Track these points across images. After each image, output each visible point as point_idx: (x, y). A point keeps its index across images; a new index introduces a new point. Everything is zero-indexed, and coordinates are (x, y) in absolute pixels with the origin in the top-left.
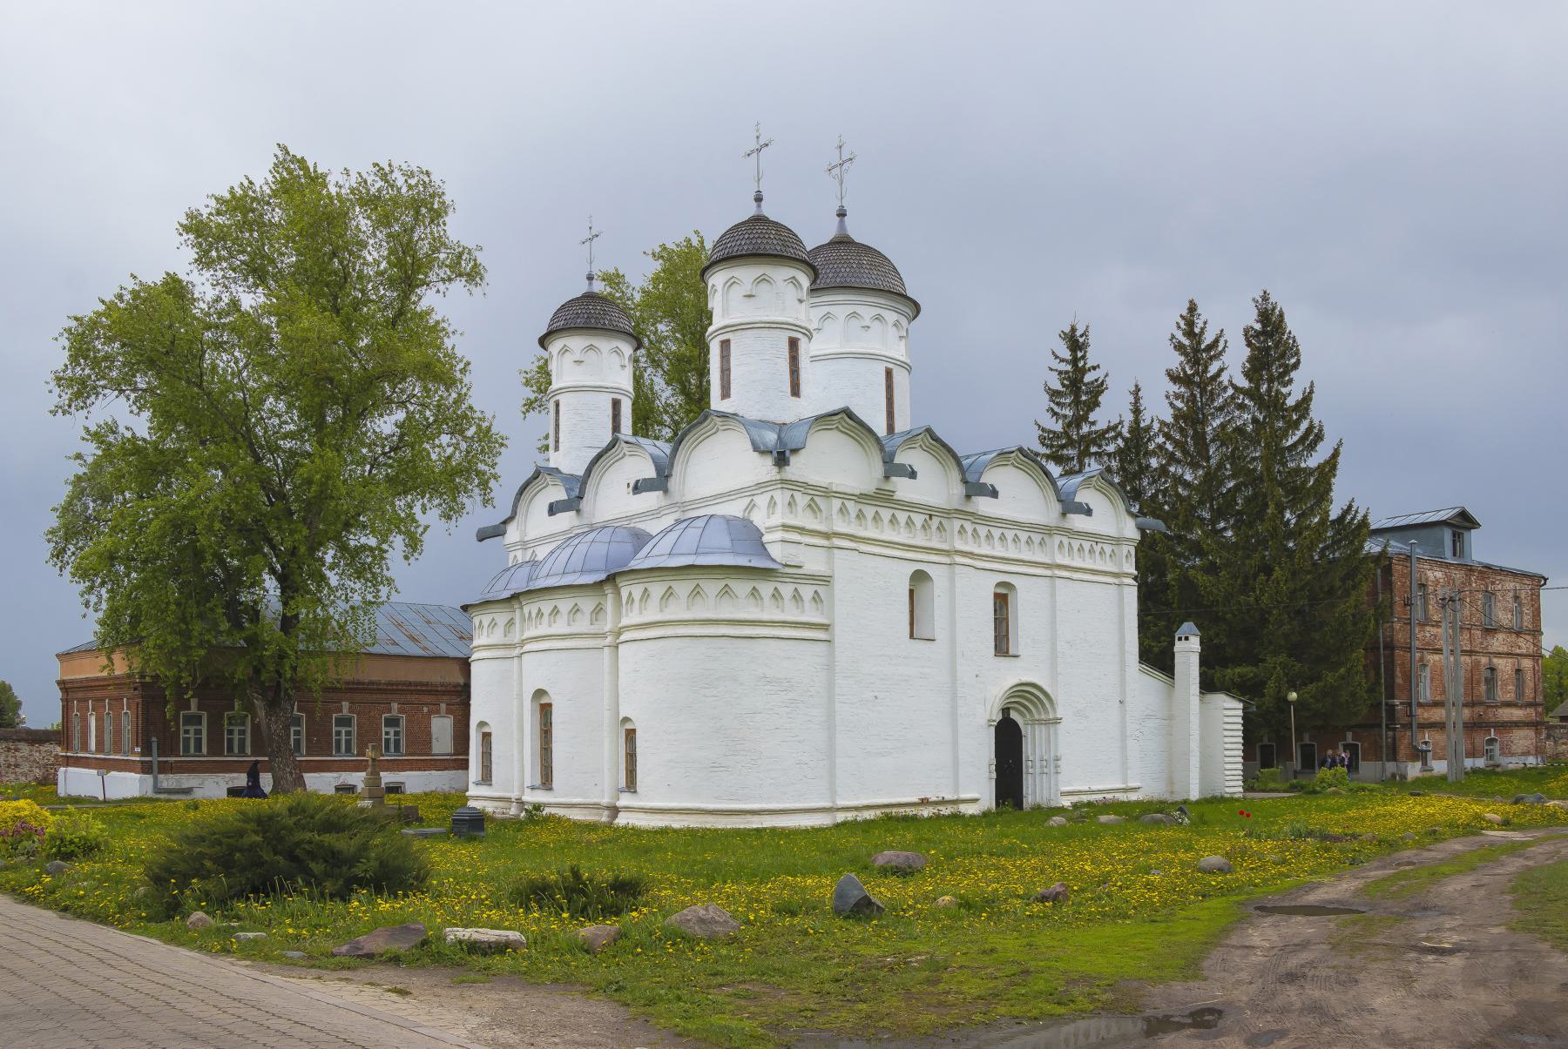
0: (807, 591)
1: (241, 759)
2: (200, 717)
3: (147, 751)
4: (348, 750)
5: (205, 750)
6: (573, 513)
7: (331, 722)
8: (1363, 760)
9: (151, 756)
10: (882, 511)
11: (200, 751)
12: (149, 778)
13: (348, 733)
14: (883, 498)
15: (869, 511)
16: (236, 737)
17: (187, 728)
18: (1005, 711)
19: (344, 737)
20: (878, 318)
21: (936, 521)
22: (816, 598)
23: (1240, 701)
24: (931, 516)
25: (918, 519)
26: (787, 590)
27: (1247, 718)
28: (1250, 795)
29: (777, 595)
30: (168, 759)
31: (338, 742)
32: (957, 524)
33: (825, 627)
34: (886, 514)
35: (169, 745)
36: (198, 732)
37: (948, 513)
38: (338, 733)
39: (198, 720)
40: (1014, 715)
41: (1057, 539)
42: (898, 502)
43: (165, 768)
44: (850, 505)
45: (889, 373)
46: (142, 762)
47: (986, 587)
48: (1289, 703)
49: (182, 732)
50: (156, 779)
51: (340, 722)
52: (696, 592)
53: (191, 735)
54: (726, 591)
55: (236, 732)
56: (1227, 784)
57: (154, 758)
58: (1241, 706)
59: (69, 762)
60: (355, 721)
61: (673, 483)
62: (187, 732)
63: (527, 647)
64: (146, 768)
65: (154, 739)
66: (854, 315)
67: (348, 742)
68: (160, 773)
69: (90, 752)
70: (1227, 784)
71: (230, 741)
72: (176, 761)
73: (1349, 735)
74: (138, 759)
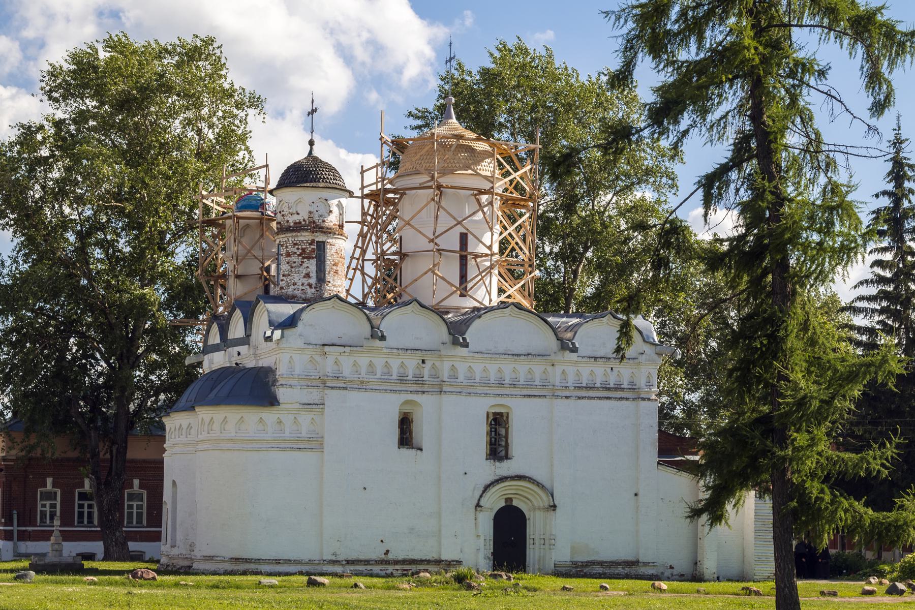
1: (88, 529)
2: (55, 493)
4: (139, 520)
5: (145, 522)
6: (247, 346)
9: (12, 525)
11: (83, 522)
12: (10, 544)
16: (86, 510)
17: (131, 503)
19: (135, 511)
21: (428, 364)
24: (423, 362)
30: (28, 528)
36: (53, 506)
38: (130, 507)
43: (23, 536)
46: (5, 531)
47: (481, 408)
50: (15, 544)
53: (48, 509)
62: (44, 506)
63: (200, 447)
65: (15, 512)
68: (19, 540)
69: (144, 527)
71: (81, 515)
72: (33, 530)
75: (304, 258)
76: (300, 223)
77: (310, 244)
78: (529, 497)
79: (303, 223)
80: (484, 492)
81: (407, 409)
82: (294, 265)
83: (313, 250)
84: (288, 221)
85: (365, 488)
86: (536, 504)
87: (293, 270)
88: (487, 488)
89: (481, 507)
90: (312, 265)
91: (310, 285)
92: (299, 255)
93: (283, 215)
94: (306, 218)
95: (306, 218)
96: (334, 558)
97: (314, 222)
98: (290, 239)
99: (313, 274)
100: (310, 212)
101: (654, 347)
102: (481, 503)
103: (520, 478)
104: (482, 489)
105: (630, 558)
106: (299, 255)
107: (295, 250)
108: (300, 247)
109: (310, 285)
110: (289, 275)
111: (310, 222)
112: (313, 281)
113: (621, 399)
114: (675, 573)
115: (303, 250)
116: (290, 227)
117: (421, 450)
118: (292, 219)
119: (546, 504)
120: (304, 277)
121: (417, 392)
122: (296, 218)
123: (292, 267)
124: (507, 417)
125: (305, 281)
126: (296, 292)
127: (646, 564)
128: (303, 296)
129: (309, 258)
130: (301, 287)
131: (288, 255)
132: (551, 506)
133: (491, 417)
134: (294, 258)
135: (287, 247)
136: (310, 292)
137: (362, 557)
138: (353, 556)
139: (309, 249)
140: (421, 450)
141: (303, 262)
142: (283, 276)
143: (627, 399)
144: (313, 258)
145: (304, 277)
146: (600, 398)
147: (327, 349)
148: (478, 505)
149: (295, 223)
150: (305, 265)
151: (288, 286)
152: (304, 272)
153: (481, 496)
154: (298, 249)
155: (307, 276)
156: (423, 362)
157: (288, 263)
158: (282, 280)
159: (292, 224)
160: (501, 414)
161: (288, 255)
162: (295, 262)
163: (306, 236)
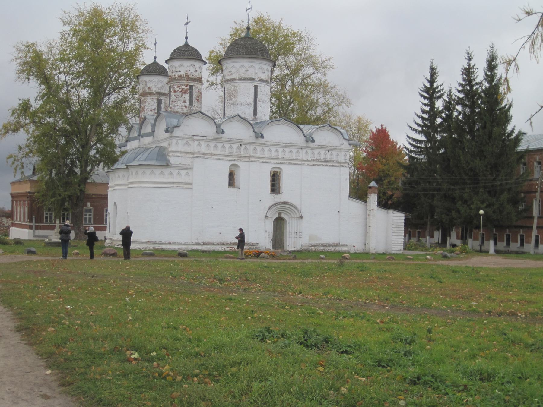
0: (183, 172)
3: (31, 221)
5: (92, 222)
7: (104, 211)
8: (486, 241)
10: (218, 144)
13: (90, 215)
14: (216, 139)
15: (212, 144)
18: (280, 214)
20: (252, 66)
21: (243, 147)
22: (187, 174)
23: (403, 213)
24: (241, 145)
25: (235, 146)
26: (175, 172)
27: (406, 220)
28: (407, 252)
29: (171, 174)
31: (86, 219)
32: (252, 147)
33: (191, 184)
34: (220, 145)
35: (39, 219)
37: (250, 143)
39: (90, 211)
40: (283, 216)
41: (304, 151)
42: (226, 141)
44: (202, 143)
45: (256, 87)
48: (480, 215)
49: (45, 214)
51: (86, 211)
52: (144, 173)
54: (152, 172)
55: (49, 214)
56: (393, 246)
57: (33, 224)
58: (404, 215)
59: (14, 225)
60: (93, 210)
61: (155, 133)
64: (30, 228)
66: (242, 66)
67: (90, 219)
70: (393, 246)
73: (521, 231)
74: (28, 224)
75: (183, 93)
76: (181, 76)
77: (186, 86)
78: (290, 212)
79: (183, 76)
80: (269, 209)
81: (233, 168)
83: (187, 90)
84: (175, 75)
85: (212, 207)
86: (293, 216)
88: (270, 207)
89: (267, 217)
90: (187, 96)
91: (186, 107)
92: (180, 92)
94: (184, 74)
95: (184, 74)
96: (197, 241)
97: (188, 76)
99: (187, 101)
100: (186, 71)
101: (347, 141)
102: (267, 215)
103: (286, 203)
104: (268, 208)
105: (336, 242)
106: (180, 92)
107: (178, 89)
109: (186, 107)
111: (186, 76)
112: (187, 104)
113: (332, 166)
114: (356, 249)
115: (183, 89)
116: (176, 78)
117: (239, 188)
118: (177, 75)
119: (298, 216)
120: (183, 102)
121: (237, 161)
122: (179, 74)
124: (280, 173)
125: (183, 104)
126: (179, 110)
127: (343, 245)
128: (182, 112)
129: (185, 93)
130: (181, 107)
131: (175, 92)
132: (300, 217)
133: (272, 173)
134: (178, 93)
135: (174, 88)
136: (186, 110)
137: (211, 241)
138: (206, 241)
139: (186, 88)
140: (239, 188)
141: (182, 95)
142: (172, 102)
143: (335, 166)
144: (187, 93)
145: (183, 102)
146: (323, 165)
147: (195, 138)
148: (266, 216)
149: (179, 76)
150: (183, 97)
151: (175, 107)
152: (183, 100)
153: (267, 212)
155: (184, 102)
156: (241, 145)
157: (175, 95)
158: (172, 104)
159: (177, 77)
160: (277, 172)
163: (184, 83)
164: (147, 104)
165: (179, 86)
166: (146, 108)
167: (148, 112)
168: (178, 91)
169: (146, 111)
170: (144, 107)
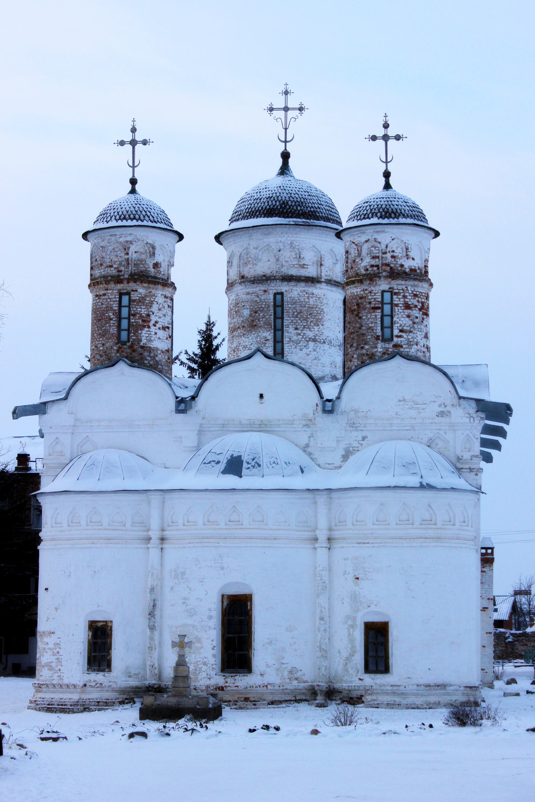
76: (415, 270)
79: (418, 271)
82: (416, 320)
84: (402, 266)
87: (415, 326)
93: (393, 257)
98: (409, 288)
107: (415, 302)
108: (420, 300)
110: (411, 332)
123: (414, 323)
131: (407, 306)
142: (401, 331)
149: (411, 270)
151: (410, 344)
154: (418, 301)
157: (408, 316)
161: (407, 306)
162: (417, 318)
164: (155, 308)
165: (415, 295)
166: (153, 319)
167: (158, 331)
168: (416, 306)
169: (153, 329)
170: (148, 315)
